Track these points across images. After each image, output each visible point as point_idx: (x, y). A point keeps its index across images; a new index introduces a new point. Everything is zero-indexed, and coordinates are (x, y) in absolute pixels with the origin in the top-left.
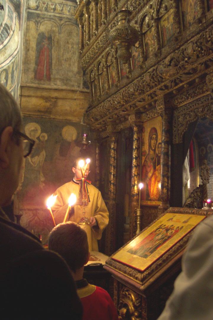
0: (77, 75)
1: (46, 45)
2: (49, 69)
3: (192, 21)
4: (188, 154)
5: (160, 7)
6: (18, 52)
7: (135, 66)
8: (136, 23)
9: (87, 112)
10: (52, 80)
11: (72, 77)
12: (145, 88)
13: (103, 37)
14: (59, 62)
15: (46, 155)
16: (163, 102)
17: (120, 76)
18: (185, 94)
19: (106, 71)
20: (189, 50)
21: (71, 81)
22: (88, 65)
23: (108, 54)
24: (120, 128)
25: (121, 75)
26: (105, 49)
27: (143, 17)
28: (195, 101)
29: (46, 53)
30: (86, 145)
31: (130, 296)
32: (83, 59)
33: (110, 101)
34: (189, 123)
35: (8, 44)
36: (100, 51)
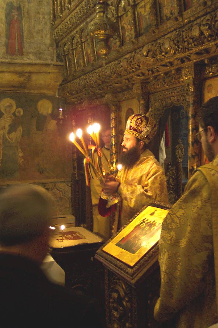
0: (50, 48)
1: (16, 17)
9: (61, 85)
10: (25, 54)
13: (76, 13)
15: (23, 131)
16: (140, 88)
17: (96, 55)
19: (81, 47)
20: (166, 46)
21: (44, 55)
22: (61, 38)
24: (96, 104)
25: (96, 54)
26: (79, 24)
28: (171, 89)
29: (16, 26)
30: (63, 119)
31: (120, 284)
33: (86, 79)
34: (165, 108)
36: (73, 26)
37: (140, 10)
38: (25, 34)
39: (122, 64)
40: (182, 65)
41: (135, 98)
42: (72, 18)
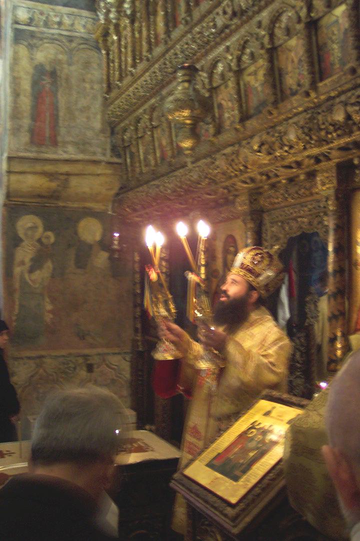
1: (48, 86)
5: (243, 53)
9: (118, 194)
13: (145, 81)
15: (54, 269)
16: (247, 202)
26: (149, 99)
29: (48, 100)
30: (118, 251)
33: (158, 186)
37: (247, 78)
38: (61, 114)
39: (217, 163)
40: (317, 167)
41: (239, 218)
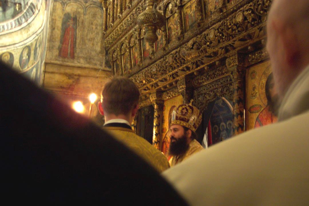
0: (100, 54)
1: (71, 25)
2: (74, 48)
3: (213, 10)
4: (207, 131)
6: (42, 30)
7: (158, 48)
8: (160, 9)
10: (76, 58)
11: (95, 56)
12: (168, 69)
13: (127, 20)
14: (82, 41)
16: (184, 82)
18: (205, 75)
20: (210, 36)
22: (111, 45)
23: (131, 36)
24: (140, 106)
26: (129, 31)
27: (166, 4)
28: (214, 82)
29: (70, 33)
32: (106, 39)
34: (208, 102)
35: (32, 23)
37: (185, 10)
38: (78, 41)
42: (122, 25)
